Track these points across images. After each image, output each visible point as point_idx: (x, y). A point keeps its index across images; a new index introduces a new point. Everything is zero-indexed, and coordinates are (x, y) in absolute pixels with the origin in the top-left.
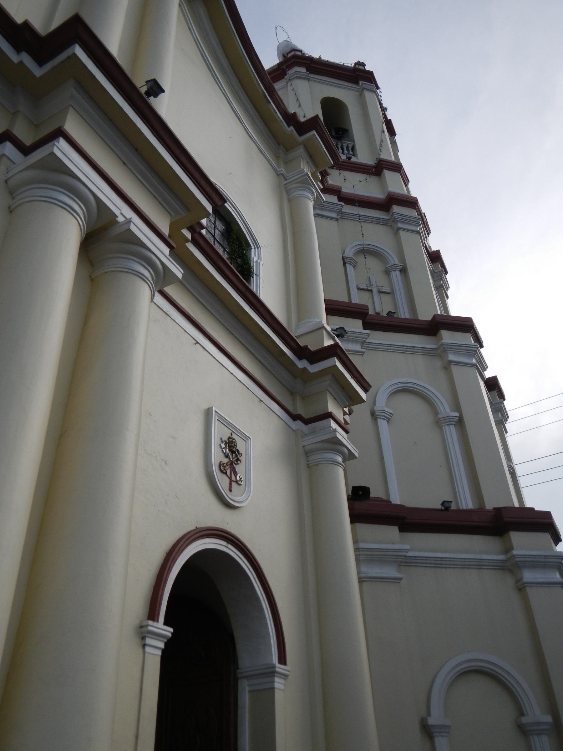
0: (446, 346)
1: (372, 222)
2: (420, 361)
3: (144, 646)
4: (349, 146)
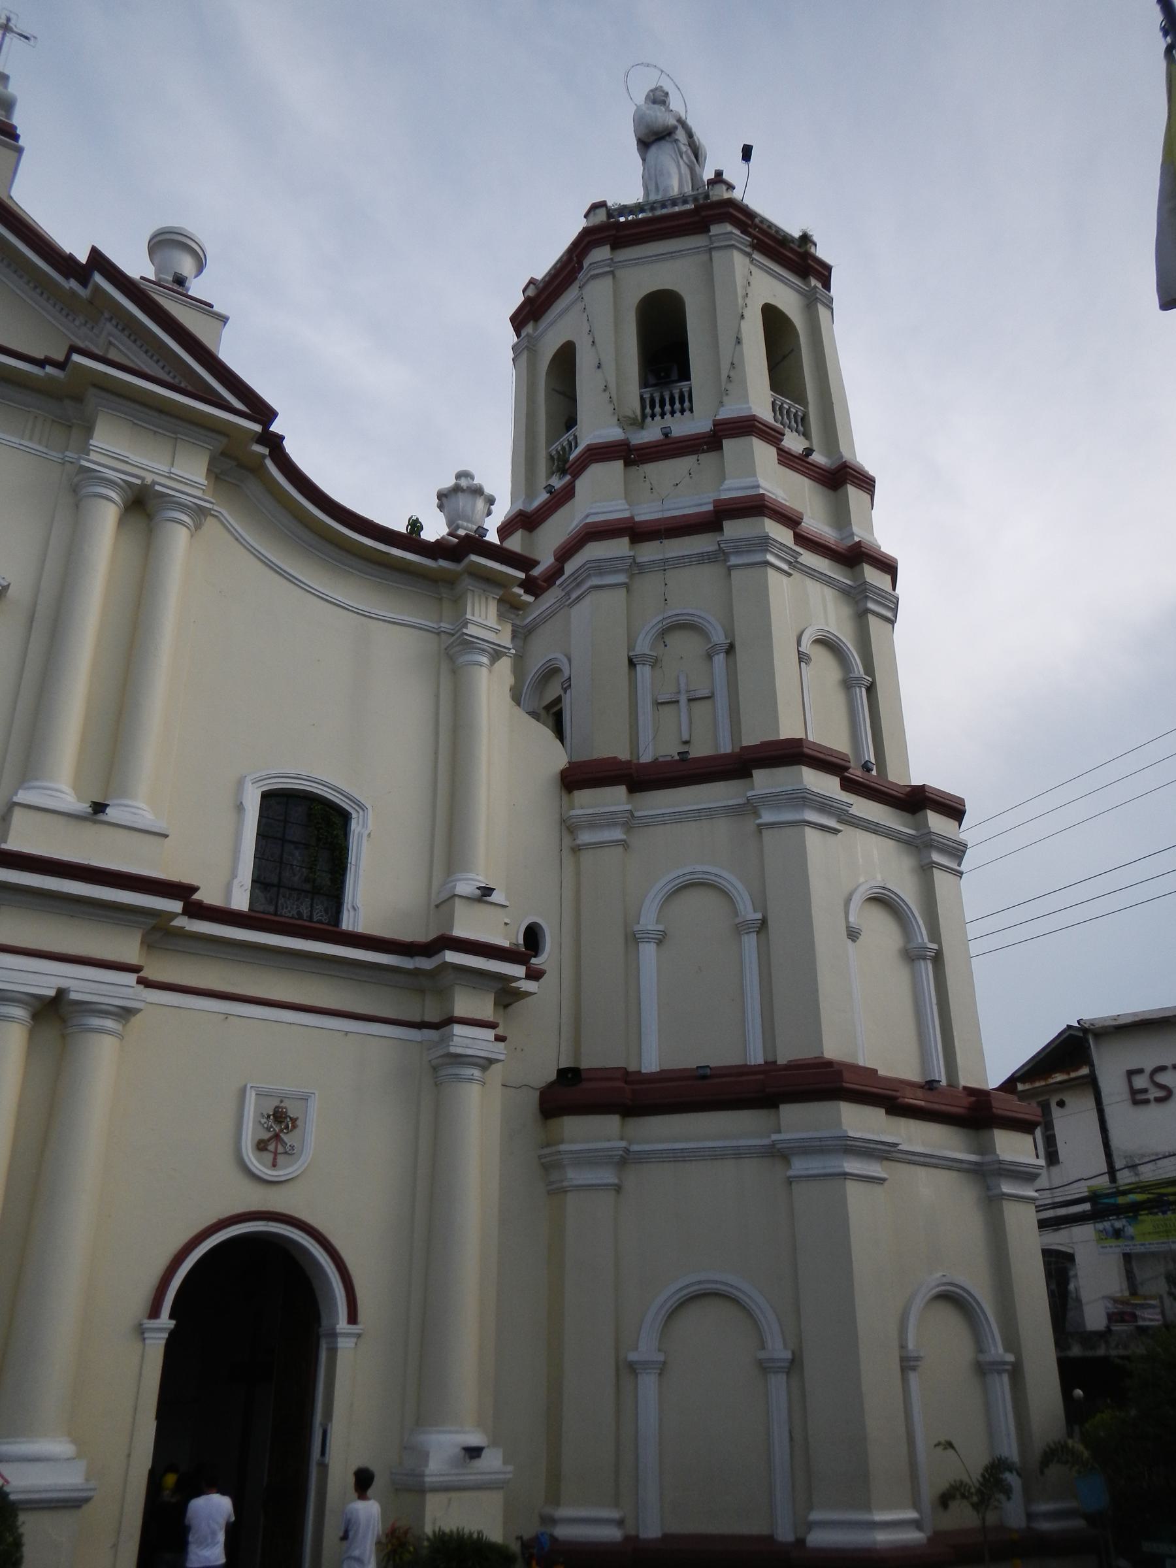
0: (754, 801)
1: (691, 564)
2: (723, 827)
3: (144, 1339)
4: (683, 390)
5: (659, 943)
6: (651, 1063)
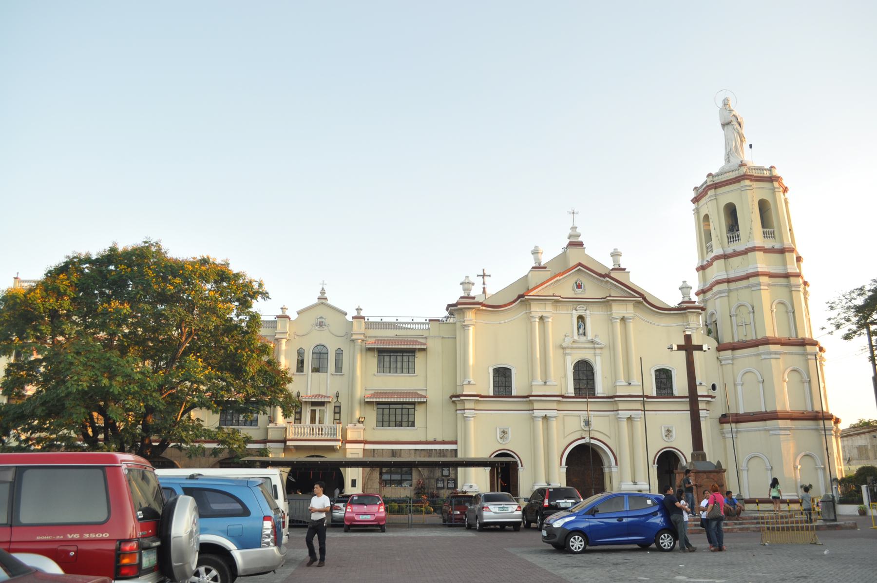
5: (742, 385)
6: (741, 412)
